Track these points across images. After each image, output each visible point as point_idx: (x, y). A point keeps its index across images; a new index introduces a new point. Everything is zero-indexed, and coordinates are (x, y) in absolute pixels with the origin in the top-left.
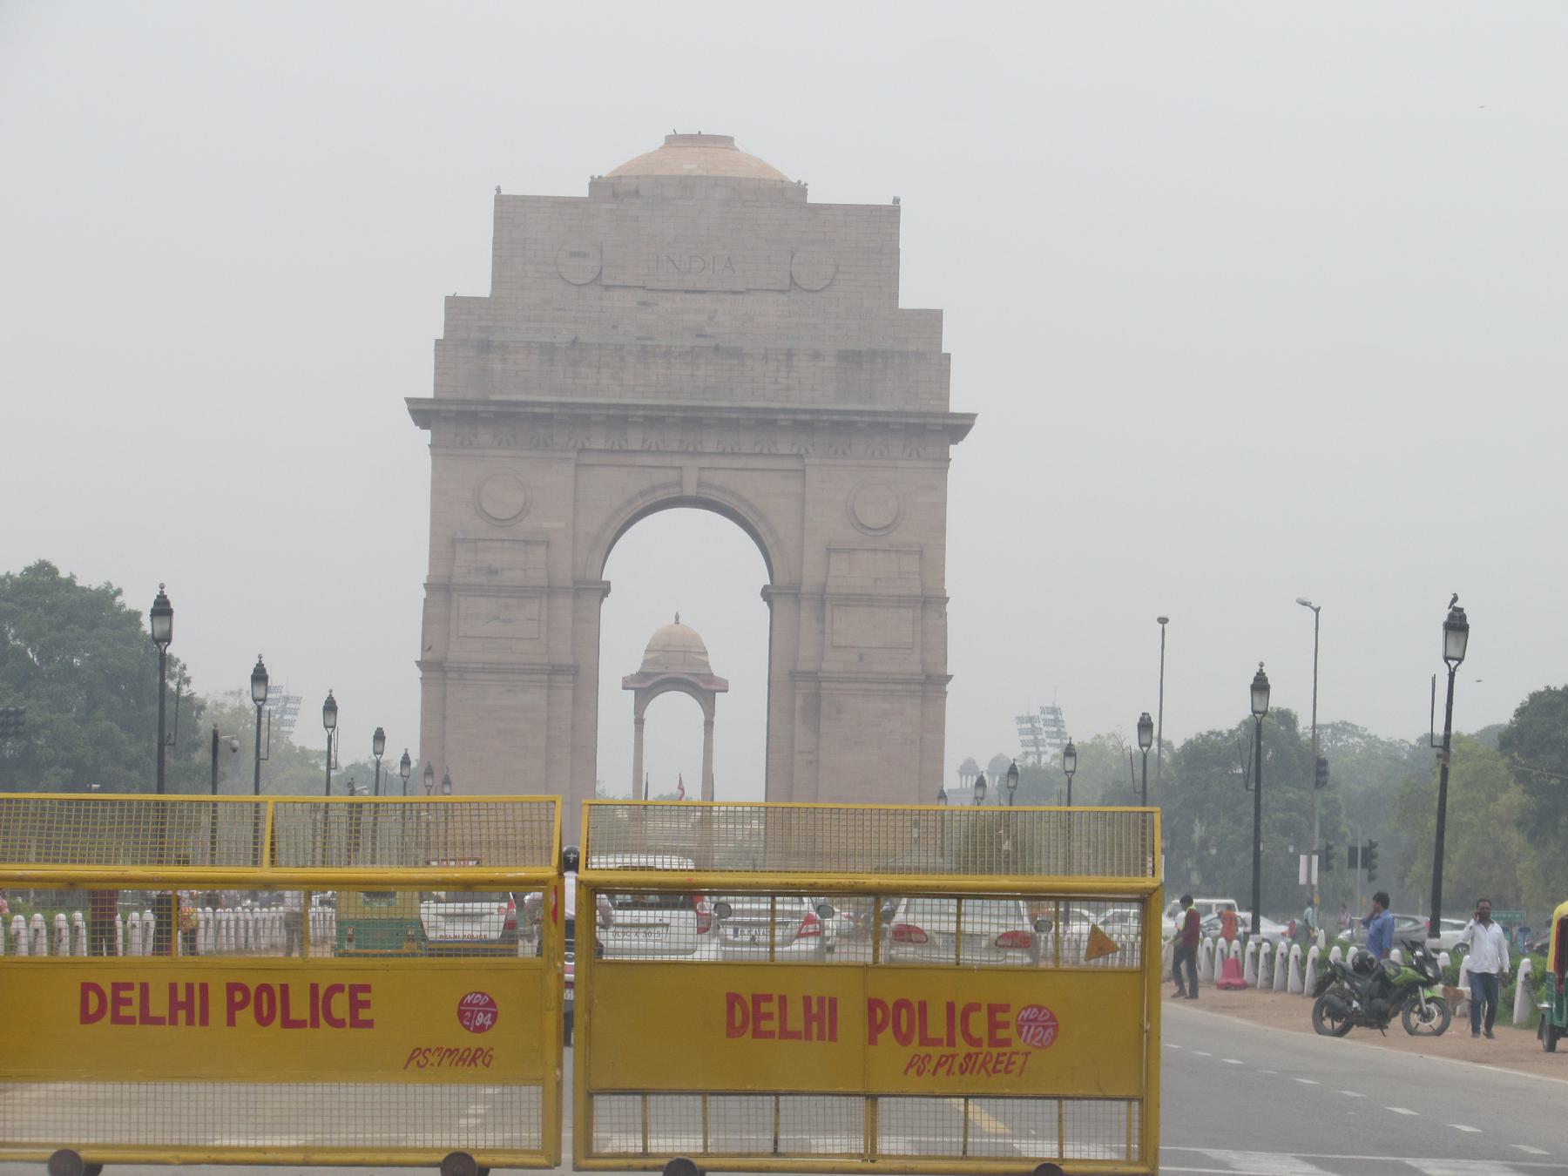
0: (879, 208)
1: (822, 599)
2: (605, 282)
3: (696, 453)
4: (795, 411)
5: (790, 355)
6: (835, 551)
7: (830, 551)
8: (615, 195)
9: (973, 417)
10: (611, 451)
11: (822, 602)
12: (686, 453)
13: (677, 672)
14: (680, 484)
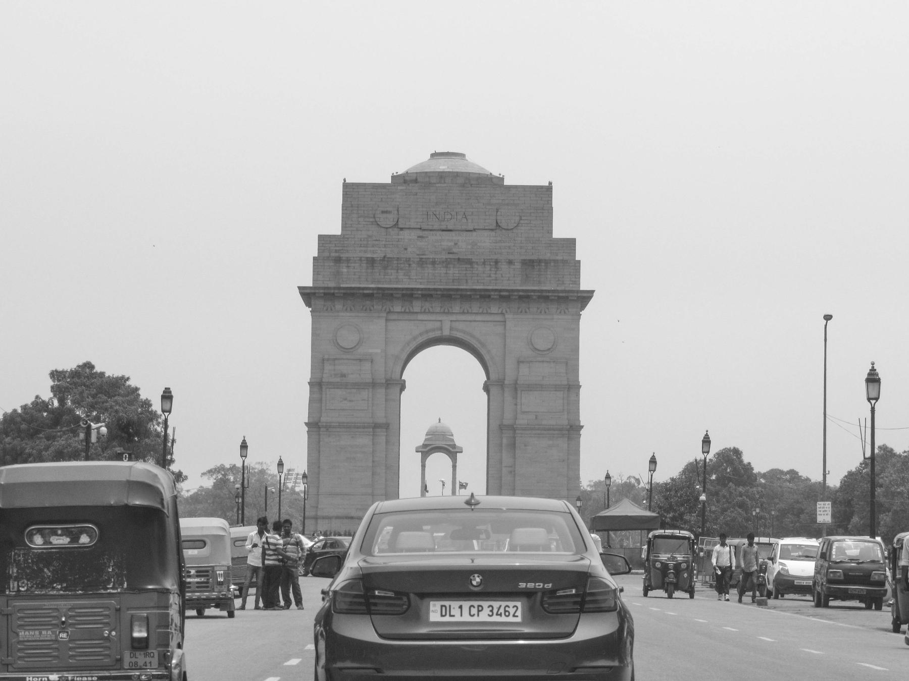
0: (542, 187)
1: (516, 388)
2: (400, 226)
3: (449, 313)
4: (500, 291)
5: (497, 262)
6: (523, 362)
7: (519, 362)
8: (405, 182)
9: (593, 292)
10: (405, 312)
11: (516, 389)
12: (444, 312)
13: (439, 444)
14: (441, 329)
